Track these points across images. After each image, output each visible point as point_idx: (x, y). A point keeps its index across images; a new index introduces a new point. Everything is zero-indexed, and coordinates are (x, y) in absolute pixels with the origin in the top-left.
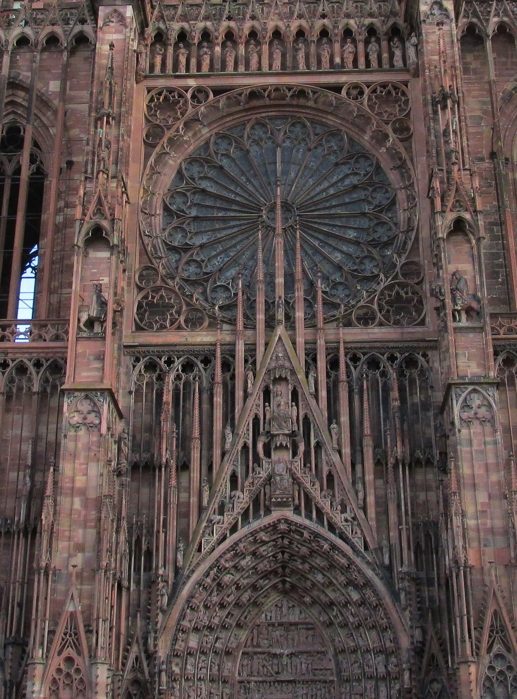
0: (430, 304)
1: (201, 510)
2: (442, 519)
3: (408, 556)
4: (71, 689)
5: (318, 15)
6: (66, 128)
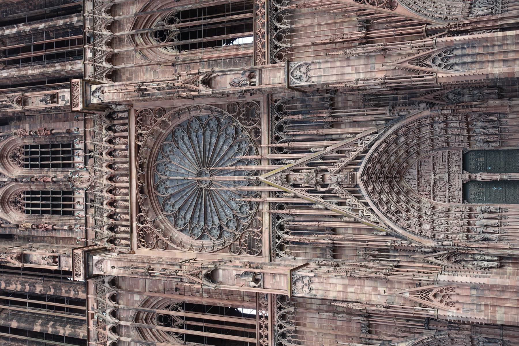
0: (249, 98)
1: (356, 222)
2: (362, 92)
4: (451, 295)
5: (101, 157)
6: (158, 291)
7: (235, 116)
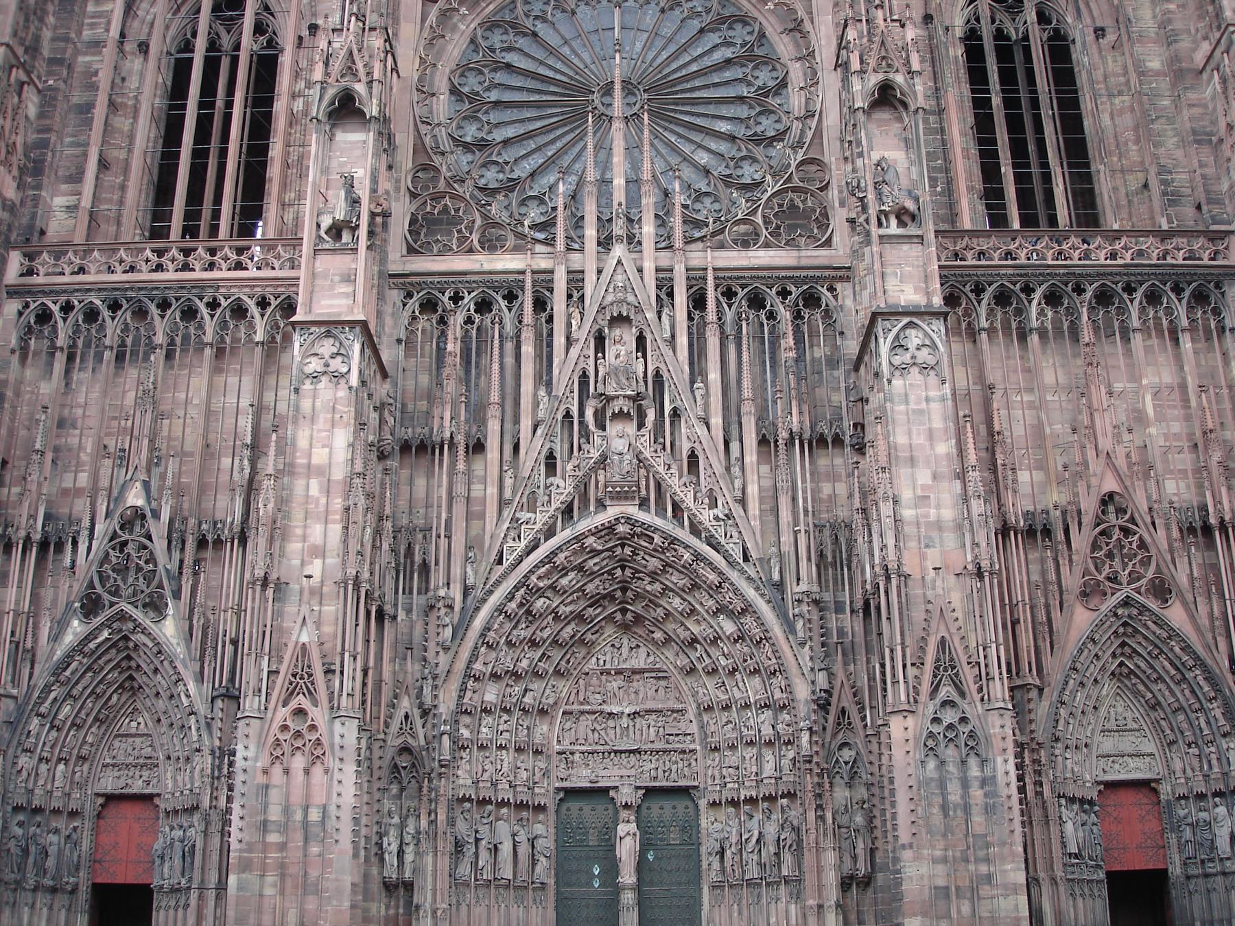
1: (502, 504)
2: (858, 518)
3: (808, 569)
7: (789, 179)
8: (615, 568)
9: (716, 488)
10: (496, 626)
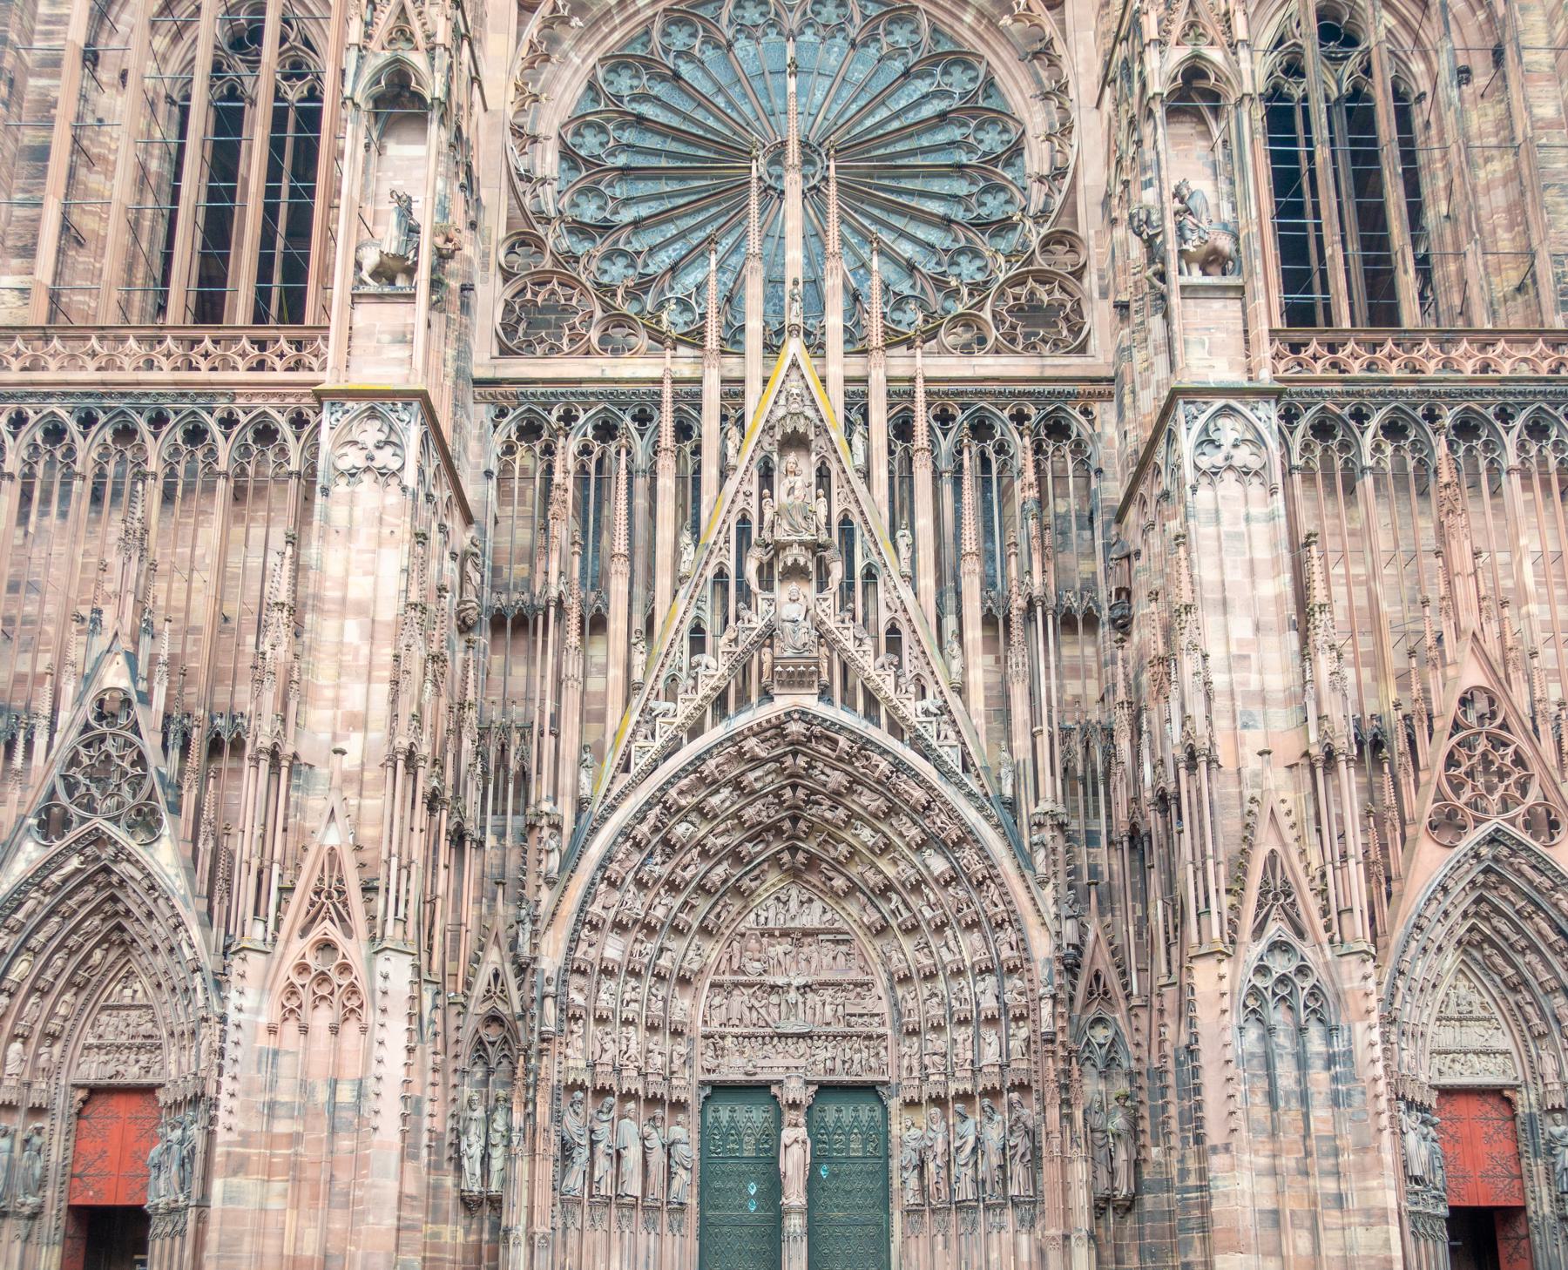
2: (1122, 719)
8: (783, 787)
9: (926, 674)
10: (621, 856)
